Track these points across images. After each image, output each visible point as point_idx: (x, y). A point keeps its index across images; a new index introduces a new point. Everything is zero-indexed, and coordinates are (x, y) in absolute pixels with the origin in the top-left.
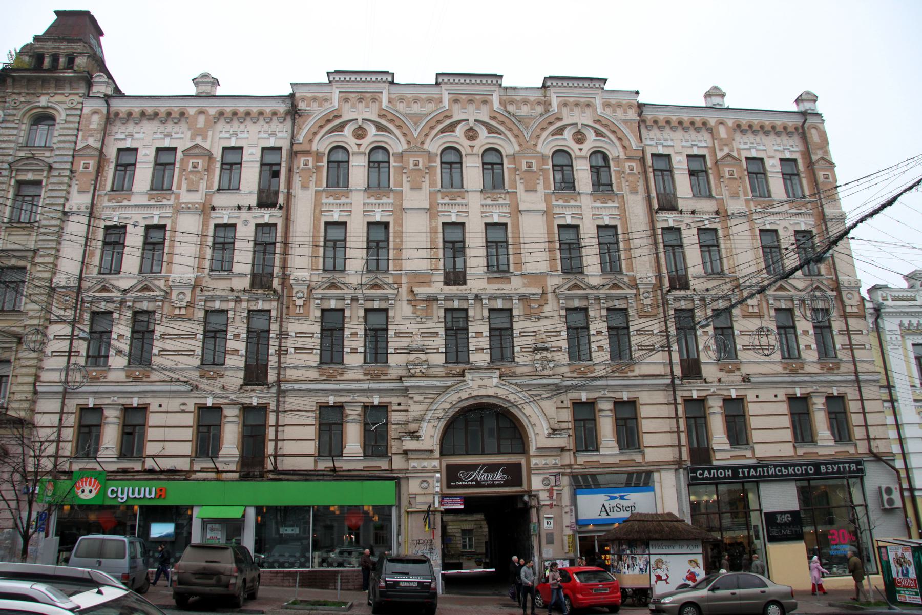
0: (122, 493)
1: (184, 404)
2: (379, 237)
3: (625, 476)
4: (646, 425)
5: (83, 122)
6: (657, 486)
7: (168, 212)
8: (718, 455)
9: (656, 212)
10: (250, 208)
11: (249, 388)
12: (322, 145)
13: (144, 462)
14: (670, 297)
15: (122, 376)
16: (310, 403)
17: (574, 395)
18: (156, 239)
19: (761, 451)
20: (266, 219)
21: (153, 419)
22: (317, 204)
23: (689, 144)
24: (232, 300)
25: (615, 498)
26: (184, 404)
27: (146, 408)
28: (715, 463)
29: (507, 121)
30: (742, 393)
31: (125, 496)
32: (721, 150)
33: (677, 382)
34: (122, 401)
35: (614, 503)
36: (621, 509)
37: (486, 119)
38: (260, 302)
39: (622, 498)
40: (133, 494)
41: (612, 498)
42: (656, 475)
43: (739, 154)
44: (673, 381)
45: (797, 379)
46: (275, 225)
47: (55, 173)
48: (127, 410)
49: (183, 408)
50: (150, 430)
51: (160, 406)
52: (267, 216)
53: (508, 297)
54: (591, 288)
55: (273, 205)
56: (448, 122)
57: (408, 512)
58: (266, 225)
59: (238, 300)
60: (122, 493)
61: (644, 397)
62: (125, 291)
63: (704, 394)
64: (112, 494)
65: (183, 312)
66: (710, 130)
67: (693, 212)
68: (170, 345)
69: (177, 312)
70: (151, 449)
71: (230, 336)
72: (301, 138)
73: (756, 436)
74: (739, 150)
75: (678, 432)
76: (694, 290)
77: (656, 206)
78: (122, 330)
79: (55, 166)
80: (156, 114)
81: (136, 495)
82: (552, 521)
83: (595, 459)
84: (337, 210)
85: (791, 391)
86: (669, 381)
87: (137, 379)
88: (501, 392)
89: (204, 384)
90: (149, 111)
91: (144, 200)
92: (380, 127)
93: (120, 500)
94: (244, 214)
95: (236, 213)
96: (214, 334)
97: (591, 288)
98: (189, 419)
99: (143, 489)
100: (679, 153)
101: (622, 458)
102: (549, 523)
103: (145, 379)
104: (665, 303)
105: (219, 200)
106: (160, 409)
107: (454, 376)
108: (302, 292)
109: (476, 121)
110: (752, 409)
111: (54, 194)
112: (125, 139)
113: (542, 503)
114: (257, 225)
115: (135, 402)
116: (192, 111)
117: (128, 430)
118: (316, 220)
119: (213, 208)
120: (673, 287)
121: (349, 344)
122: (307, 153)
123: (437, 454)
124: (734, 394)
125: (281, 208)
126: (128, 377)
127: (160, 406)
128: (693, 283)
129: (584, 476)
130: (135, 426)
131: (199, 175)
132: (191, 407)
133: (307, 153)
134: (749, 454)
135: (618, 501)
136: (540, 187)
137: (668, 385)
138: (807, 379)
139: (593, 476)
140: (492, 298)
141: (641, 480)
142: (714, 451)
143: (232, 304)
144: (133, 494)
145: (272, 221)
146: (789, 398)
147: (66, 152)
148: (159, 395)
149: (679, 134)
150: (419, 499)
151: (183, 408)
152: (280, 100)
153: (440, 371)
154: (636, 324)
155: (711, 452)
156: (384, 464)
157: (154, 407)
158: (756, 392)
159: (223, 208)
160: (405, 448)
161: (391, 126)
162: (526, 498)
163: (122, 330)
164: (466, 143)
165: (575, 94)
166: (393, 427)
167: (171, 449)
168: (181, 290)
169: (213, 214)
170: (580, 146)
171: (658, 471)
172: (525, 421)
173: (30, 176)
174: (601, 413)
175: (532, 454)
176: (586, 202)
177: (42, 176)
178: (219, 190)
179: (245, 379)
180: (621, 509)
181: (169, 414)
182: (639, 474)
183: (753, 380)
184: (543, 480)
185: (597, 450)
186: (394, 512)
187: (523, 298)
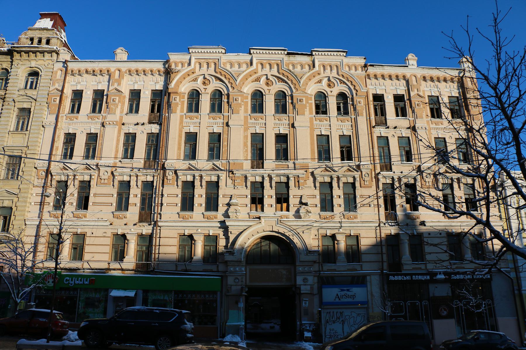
1: (105, 233)
2: (216, 140)
5: (54, 75)
6: (368, 284)
8: (405, 267)
9: (374, 127)
10: (143, 124)
11: (141, 224)
12: (185, 88)
14: (380, 177)
16: (175, 234)
19: (430, 266)
21: (88, 241)
22: (181, 122)
25: (345, 290)
26: (105, 233)
29: (289, 76)
33: (382, 225)
35: (343, 293)
36: (347, 296)
39: (348, 290)
41: (342, 290)
42: (368, 278)
43: (424, 94)
44: (379, 225)
49: (104, 234)
54: (334, 171)
57: (227, 296)
65: (106, 181)
67: (395, 128)
70: (86, 257)
72: (172, 85)
73: (428, 257)
74: (424, 91)
76: (394, 172)
77: (374, 124)
82: (307, 302)
86: (377, 225)
88: (281, 231)
89: (116, 221)
90: (90, 69)
91: (85, 119)
97: (334, 171)
98: (109, 241)
102: (305, 303)
104: (377, 180)
106: (92, 235)
109: (272, 75)
113: (302, 292)
116: (112, 70)
118: (180, 131)
120: (382, 170)
122: (176, 93)
123: (244, 263)
132: (109, 234)
133: (176, 93)
134: (423, 267)
135: (346, 292)
136: (307, 112)
141: (360, 281)
147: (44, 92)
149: (388, 81)
150: (234, 288)
151: (104, 234)
154: (359, 192)
156: (214, 268)
159: (129, 124)
160: (226, 260)
161: (223, 78)
162: (294, 289)
164: (266, 88)
167: (97, 257)
170: (331, 90)
175: (297, 264)
176: (334, 120)
179: (139, 219)
180: (347, 296)
181: (96, 238)
183: (427, 224)
184: (304, 279)
186: (219, 293)
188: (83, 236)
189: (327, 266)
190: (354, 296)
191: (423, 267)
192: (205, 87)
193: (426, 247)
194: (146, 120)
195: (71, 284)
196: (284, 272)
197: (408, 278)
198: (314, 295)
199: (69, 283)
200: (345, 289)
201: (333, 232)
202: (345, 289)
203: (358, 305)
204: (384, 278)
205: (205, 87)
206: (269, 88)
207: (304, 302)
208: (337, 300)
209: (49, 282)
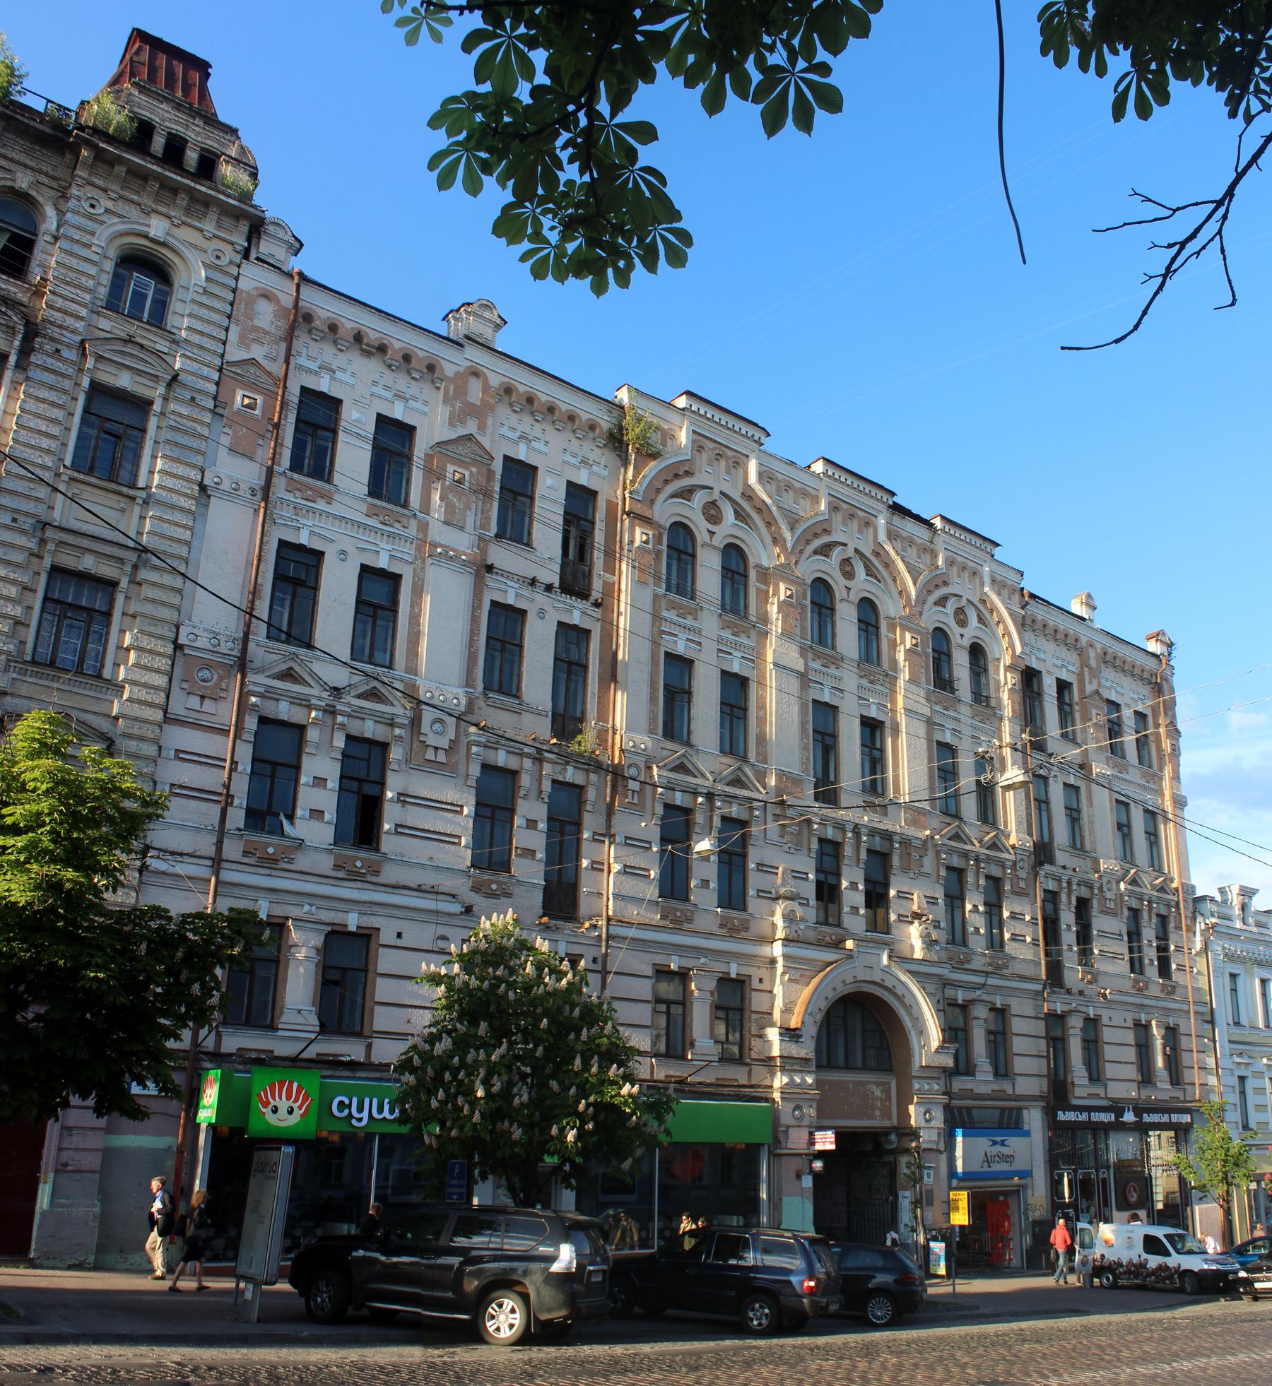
0: (360, 1110)
1: (444, 938)
3: (997, 1112)
4: (1018, 1045)
5: (241, 308)
7: (408, 551)
8: (1078, 1092)
10: (549, 588)
13: (369, 1046)
15: (325, 863)
16: (643, 963)
17: (949, 992)
18: (379, 596)
20: (576, 618)
23: (1059, 663)
24: (528, 756)
27: (369, 937)
28: (1075, 1102)
30: (1100, 1012)
31: (365, 1115)
32: (1091, 682)
34: (327, 916)
37: (868, 554)
38: (570, 769)
39: (1003, 1143)
40: (380, 1110)
41: (995, 1143)
42: (1025, 1112)
45: (1146, 1002)
46: (588, 632)
47: (178, 391)
48: (336, 937)
49: (442, 944)
50: (379, 981)
51: (399, 935)
52: (577, 613)
53: (887, 836)
55: (584, 595)
56: (826, 539)
58: (575, 627)
59: (539, 760)
60: (360, 1110)
61: (1019, 1006)
62: (336, 691)
63: (1066, 1008)
64: (341, 1111)
65: (441, 757)
66: (1081, 652)
68: (415, 817)
69: (430, 755)
70: (382, 1019)
71: (518, 821)
75: (1048, 1057)
78: (321, 768)
79: (182, 377)
80: (382, 349)
81: (386, 1114)
83: (969, 1086)
84: (683, 635)
85: (1137, 1016)
87: (354, 876)
92: (740, 515)
93: (354, 1122)
94: (541, 599)
95: (526, 592)
96: (494, 811)
99: (367, 1101)
100: (1050, 673)
101: (996, 1087)
103: (369, 878)
105: (502, 555)
106: (400, 943)
107: (828, 945)
108: (637, 766)
109: (856, 551)
110: (1107, 1034)
111: (179, 438)
112: (316, 373)
114: (560, 624)
115: (353, 922)
117: (335, 976)
119: (490, 568)
121: (308, 797)
124: (1092, 1012)
125: (597, 604)
126: (337, 867)
127: (399, 935)
128: (1061, 857)
129: (960, 1109)
130: (344, 970)
131: (464, 499)
135: (998, 1148)
137: (1037, 992)
138: (1152, 1003)
139: (969, 1109)
140: (873, 832)
142: (1073, 1084)
143: (528, 763)
144: (380, 1110)
145: (585, 625)
146: (1135, 1025)
148: (397, 912)
151: (442, 944)
152: (604, 407)
153: (811, 935)
155: (1069, 1086)
157: (387, 936)
158: (1113, 1014)
163: (321, 768)
164: (842, 581)
165: (967, 552)
166: (754, 1016)
168: (439, 714)
169: (489, 579)
171: (1027, 1108)
172: (907, 1022)
173: (124, 381)
174: (975, 1022)
177: (156, 393)
178: (497, 536)
179: (544, 908)
182: (1011, 1110)
185: (974, 1075)
187: (906, 842)
188: (366, 937)
189: (959, 1084)
190: (1008, 1159)
191: (1101, 1092)
192: (713, 528)
193: (1016, 1040)
194: (556, 581)
195: (360, 1120)
196: (878, 1093)
197: (1084, 1117)
198: (941, 1153)
199: (350, 1116)
200: (998, 1139)
201: (971, 995)
202: (998, 1139)
203: (1012, 1178)
204: (1050, 1113)
205: (713, 528)
206: (849, 584)
207: (926, 1172)
208: (986, 1169)
209: (275, 1110)
